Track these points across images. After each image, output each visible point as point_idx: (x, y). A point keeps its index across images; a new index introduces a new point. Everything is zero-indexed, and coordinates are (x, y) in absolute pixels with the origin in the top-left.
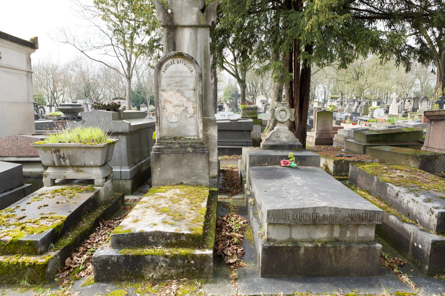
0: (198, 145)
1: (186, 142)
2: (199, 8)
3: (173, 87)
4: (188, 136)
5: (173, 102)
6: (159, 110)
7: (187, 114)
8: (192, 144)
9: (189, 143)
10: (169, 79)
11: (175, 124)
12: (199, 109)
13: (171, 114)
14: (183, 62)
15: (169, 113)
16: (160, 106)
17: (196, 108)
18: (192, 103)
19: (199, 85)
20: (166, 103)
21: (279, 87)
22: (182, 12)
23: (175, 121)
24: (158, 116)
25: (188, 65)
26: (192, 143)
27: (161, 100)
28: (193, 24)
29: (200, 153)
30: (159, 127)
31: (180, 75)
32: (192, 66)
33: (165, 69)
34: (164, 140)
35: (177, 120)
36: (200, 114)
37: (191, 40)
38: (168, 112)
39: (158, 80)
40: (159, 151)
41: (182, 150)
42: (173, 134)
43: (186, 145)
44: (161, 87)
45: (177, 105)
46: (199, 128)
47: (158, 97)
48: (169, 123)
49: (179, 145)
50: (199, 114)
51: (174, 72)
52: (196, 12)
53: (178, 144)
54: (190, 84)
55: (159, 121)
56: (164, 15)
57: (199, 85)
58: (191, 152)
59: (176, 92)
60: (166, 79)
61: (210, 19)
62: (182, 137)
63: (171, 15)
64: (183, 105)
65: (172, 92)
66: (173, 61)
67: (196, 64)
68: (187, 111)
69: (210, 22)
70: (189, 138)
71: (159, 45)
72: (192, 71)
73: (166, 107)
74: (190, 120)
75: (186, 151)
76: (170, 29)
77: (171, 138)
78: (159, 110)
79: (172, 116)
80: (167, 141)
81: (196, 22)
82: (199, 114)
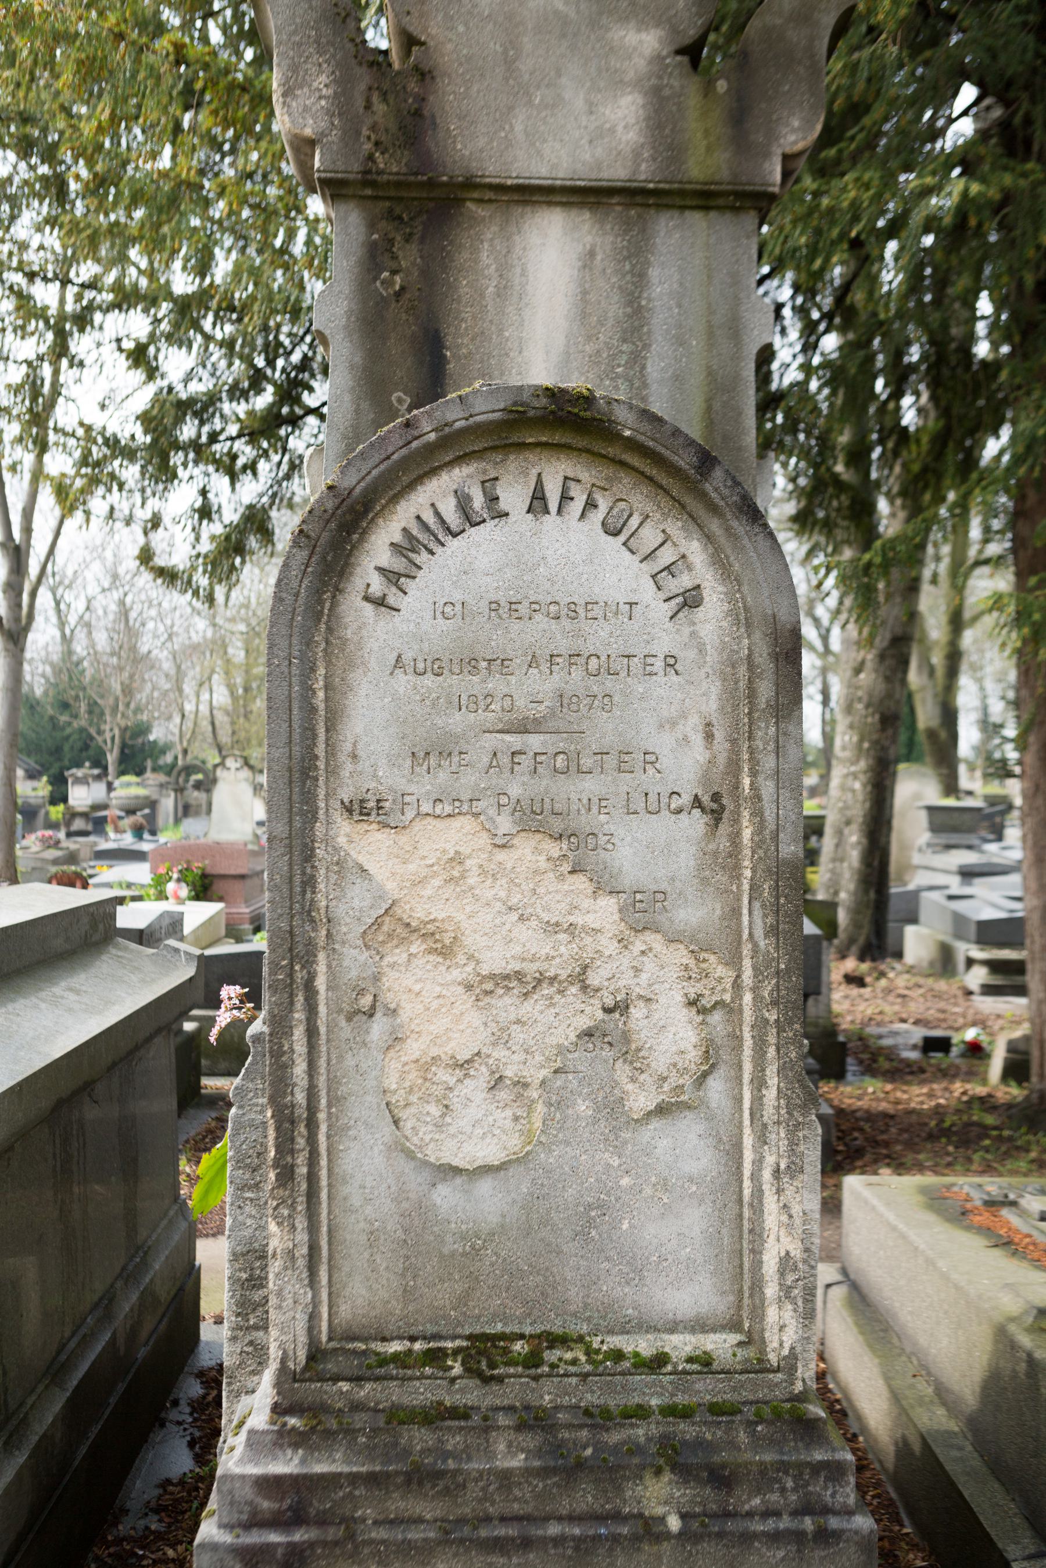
0: (756, 1439)
1: (614, 1402)
2: (674, 30)
3: (470, 779)
4: (624, 1329)
5: (472, 941)
6: (312, 1033)
7: (622, 1072)
8: (687, 1430)
9: (641, 1412)
10: (429, 680)
11: (485, 1186)
12: (760, 1025)
13: (445, 1076)
14: (591, 504)
15: (426, 1066)
16: (321, 983)
17: (732, 1010)
18: (680, 955)
19: (769, 762)
20: (399, 956)
21: (881, 701)
22: (510, 64)
23: (490, 1152)
24: (300, 1097)
25: (650, 536)
26: (685, 1413)
27: (340, 910)
28: (617, 173)
29: (775, 1538)
30: (301, 1223)
31: (563, 645)
32: (696, 550)
33: (392, 577)
34: (357, 1379)
35: (515, 1143)
36: (773, 1080)
37: (584, 315)
38: (414, 1048)
39: (308, 691)
40: (295, 1518)
41: (565, 1507)
42: (463, 1300)
43: (614, 1437)
44: (347, 768)
45: (519, 976)
46: (757, 1234)
47: (310, 883)
48: (416, 1181)
49: (530, 1440)
50: (758, 1082)
51: (494, 606)
52: (638, 65)
53: (521, 1427)
54: (663, 744)
55: (301, 1159)
56: (343, 83)
57: (769, 762)
58: (674, 1523)
59: (505, 824)
60: (403, 682)
61: (772, 136)
62: (562, 1341)
63: (413, 86)
64: (580, 978)
65: (466, 823)
66: (489, 484)
67: (739, 527)
68: (626, 1037)
69: (767, 155)
70: (644, 1346)
71: (214, 438)
72: (691, 600)
73: (389, 998)
74: (663, 1144)
75: (617, 1517)
76: (392, 216)
77: (435, 1357)
78: (312, 1033)
79: (455, 1102)
80: (395, 1394)
81: (637, 154)
82: (758, 1082)
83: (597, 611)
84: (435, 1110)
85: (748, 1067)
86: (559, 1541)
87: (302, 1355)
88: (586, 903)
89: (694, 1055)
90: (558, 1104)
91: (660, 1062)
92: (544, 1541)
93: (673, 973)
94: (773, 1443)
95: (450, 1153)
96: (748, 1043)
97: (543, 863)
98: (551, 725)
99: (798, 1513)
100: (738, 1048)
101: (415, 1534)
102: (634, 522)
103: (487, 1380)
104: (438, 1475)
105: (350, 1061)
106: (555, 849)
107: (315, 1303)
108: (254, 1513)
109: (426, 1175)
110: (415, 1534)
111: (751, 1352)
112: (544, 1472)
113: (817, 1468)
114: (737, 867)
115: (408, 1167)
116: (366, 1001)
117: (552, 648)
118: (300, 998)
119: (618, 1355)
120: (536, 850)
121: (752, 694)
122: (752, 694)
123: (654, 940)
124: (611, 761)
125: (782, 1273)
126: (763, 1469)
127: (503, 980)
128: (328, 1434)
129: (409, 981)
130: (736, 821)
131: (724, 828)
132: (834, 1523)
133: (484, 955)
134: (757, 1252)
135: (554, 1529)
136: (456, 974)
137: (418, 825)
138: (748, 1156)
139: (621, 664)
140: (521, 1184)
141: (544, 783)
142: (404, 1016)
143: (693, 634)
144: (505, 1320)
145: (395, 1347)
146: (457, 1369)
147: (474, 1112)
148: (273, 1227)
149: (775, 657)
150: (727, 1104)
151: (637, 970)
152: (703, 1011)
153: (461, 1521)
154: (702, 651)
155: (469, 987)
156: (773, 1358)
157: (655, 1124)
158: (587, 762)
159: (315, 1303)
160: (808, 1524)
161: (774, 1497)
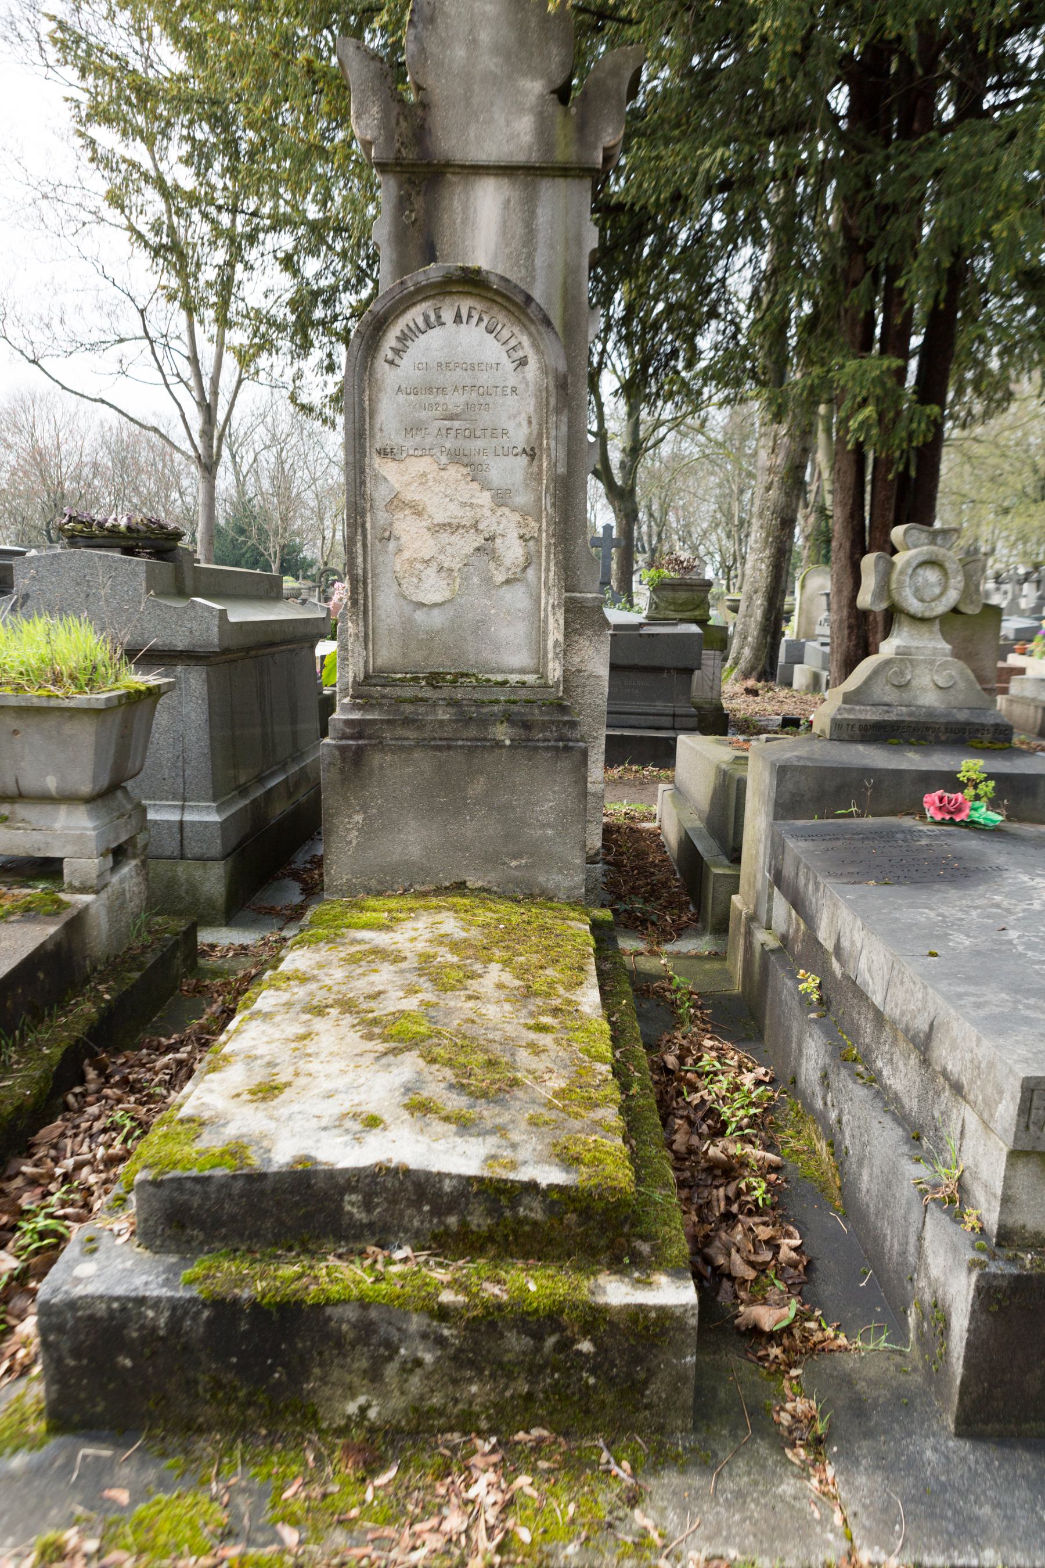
0: (542, 713)
1: (486, 698)
2: (550, 81)
3: (429, 440)
4: (492, 671)
5: (430, 509)
6: (365, 546)
7: (492, 565)
8: (514, 708)
9: (497, 702)
10: (412, 397)
11: (436, 612)
12: (549, 545)
13: (419, 566)
14: (480, 319)
15: (412, 562)
16: (368, 526)
17: (538, 540)
18: (516, 517)
19: (553, 433)
20: (401, 515)
21: (782, 509)
22: (467, 100)
23: (438, 598)
24: (360, 572)
25: (506, 334)
26: (514, 702)
27: (376, 495)
28: (520, 158)
29: (547, 748)
30: (361, 623)
31: (468, 382)
32: (525, 340)
33: (397, 351)
34: (384, 686)
35: (448, 595)
36: (552, 568)
37: (504, 234)
38: (406, 554)
39: (361, 401)
40: (360, 736)
41: (465, 735)
42: (426, 659)
43: (485, 710)
44: (378, 435)
45: (450, 524)
46: (546, 633)
47: (363, 483)
48: (407, 609)
49: (452, 710)
50: (548, 570)
51: (439, 365)
52: (531, 100)
53: (448, 705)
54: (510, 426)
55: (361, 597)
56: (385, 112)
57: (553, 433)
58: (508, 742)
59: (444, 460)
60: (401, 398)
61: (598, 137)
62: (467, 675)
63: (420, 112)
64: (475, 526)
65: (428, 459)
66: (437, 310)
67: (543, 329)
68: (493, 551)
69: (595, 148)
70: (500, 678)
71: (335, 318)
72: (523, 362)
73: (396, 533)
74: (508, 596)
75: (485, 739)
76: (411, 182)
77: (416, 679)
78: (365, 546)
79: (423, 577)
80: (399, 692)
81: (530, 148)
82: (548, 570)
83: (483, 367)
84: (415, 580)
85: (543, 564)
86: (462, 747)
87: (362, 676)
88: (478, 494)
89: (522, 559)
90: (466, 578)
91: (508, 562)
92: (456, 747)
93: (513, 525)
94: (548, 714)
95: (421, 597)
96: (544, 554)
97: (460, 477)
98: (463, 416)
99: (557, 740)
100: (540, 557)
101: (406, 743)
102: (499, 327)
103: (435, 687)
104: (415, 721)
105: (381, 559)
106: (465, 471)
107: (367, 656)
108: (344, 733)
109: (411, 607)
110: (406, 743)
111: (542, 681)
112: (456, 721)
113: (565, 723)
114: (541, 479)
115: (404, 603)
116: (387, 534)
117: (464, 383)
118: (359, 530)
119: (489, 680)
120: (457, 471)
121: (548, 404)
122: (548, 404)
123: (506, 510)
124: (488, 433)
125: (555, 647)
126: (544, 723)
127: (443, 526)
128: (372, 705)
129: (404, 526)
130: (541, 459)
131: (535, 462)
132: (571, 744)
133: (436, 516)
134: (545, 640)
135: (460, 743)
136: (424, 523)
137: (408, 460)
138: (543, 601)
139: (492, 391)
140: (450, 611)
141: (460, 443)
142: (402, 541)
143: (524, 378)
144: (444, 667)
145: (399, 676)
146: (424, 683)
147: (431, 581)
148: (350, 624)
149: (556, 387)
150: (535, 580)
151: (499, 523)
152: (526, 541)
153: (424, 739)
154: (527, 384)
155: (429, 529)
156: (551, 683)
157: (505, 587)
158: (478, 433)
159: (367, 656)
160: (561, 744)
161: (548, 734)
